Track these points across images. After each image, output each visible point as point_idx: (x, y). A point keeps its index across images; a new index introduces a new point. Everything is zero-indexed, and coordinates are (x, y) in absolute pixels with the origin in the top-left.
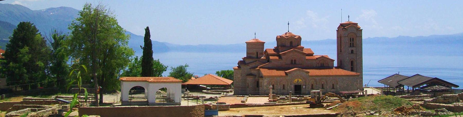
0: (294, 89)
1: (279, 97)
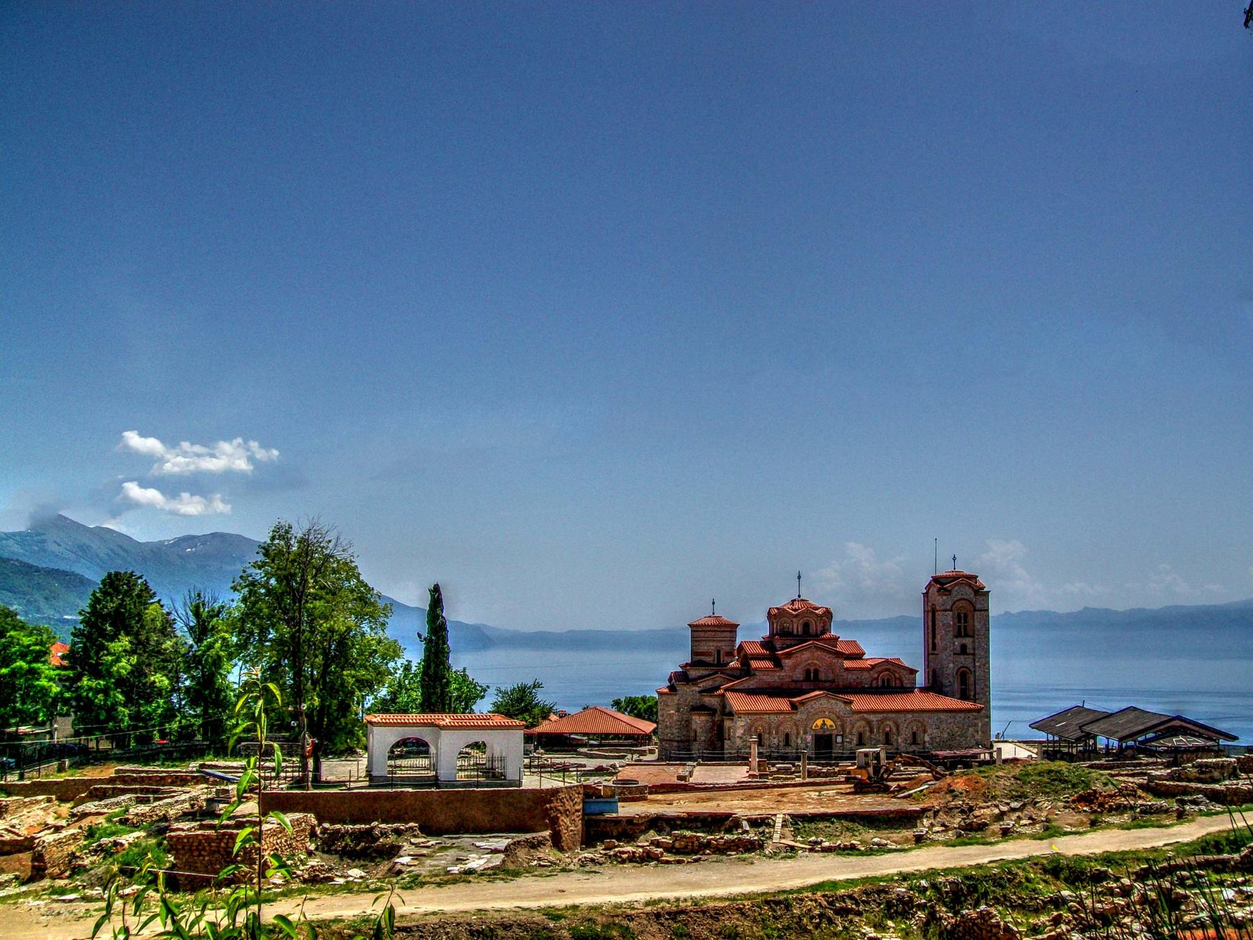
1: (773, 765)
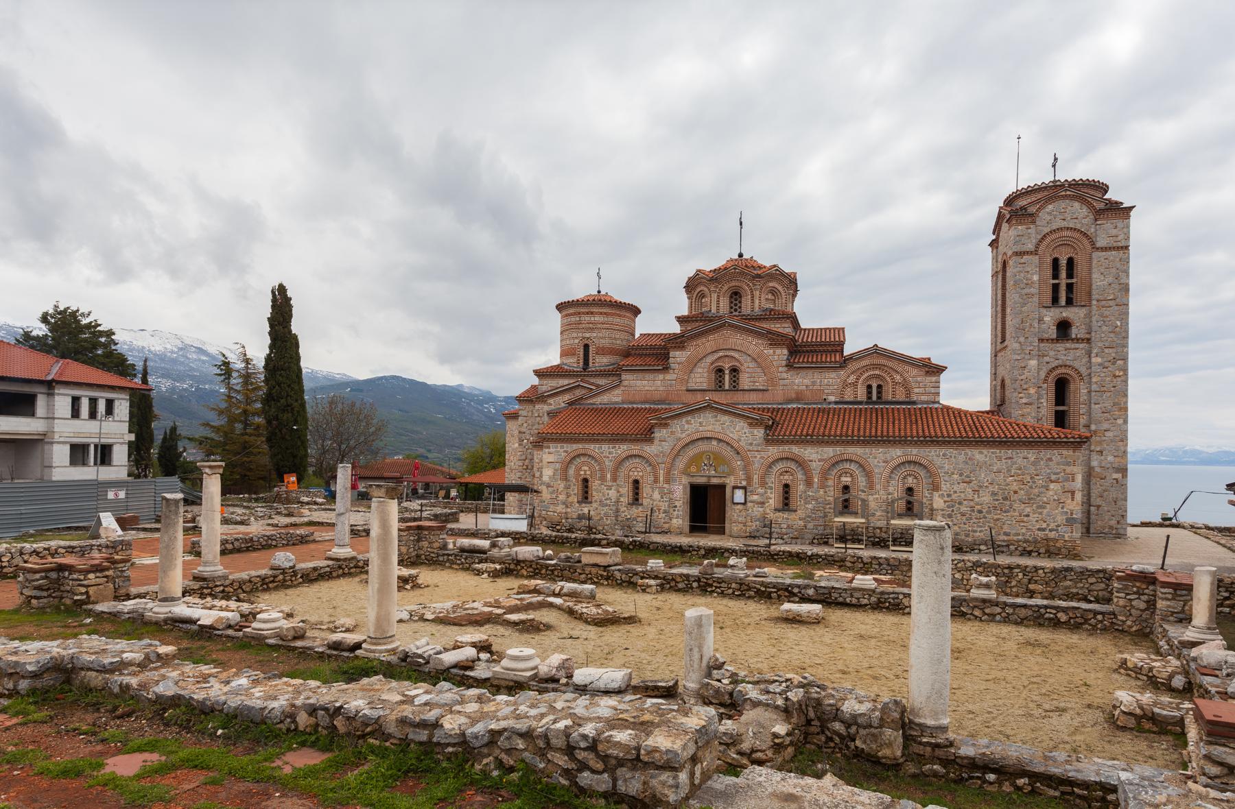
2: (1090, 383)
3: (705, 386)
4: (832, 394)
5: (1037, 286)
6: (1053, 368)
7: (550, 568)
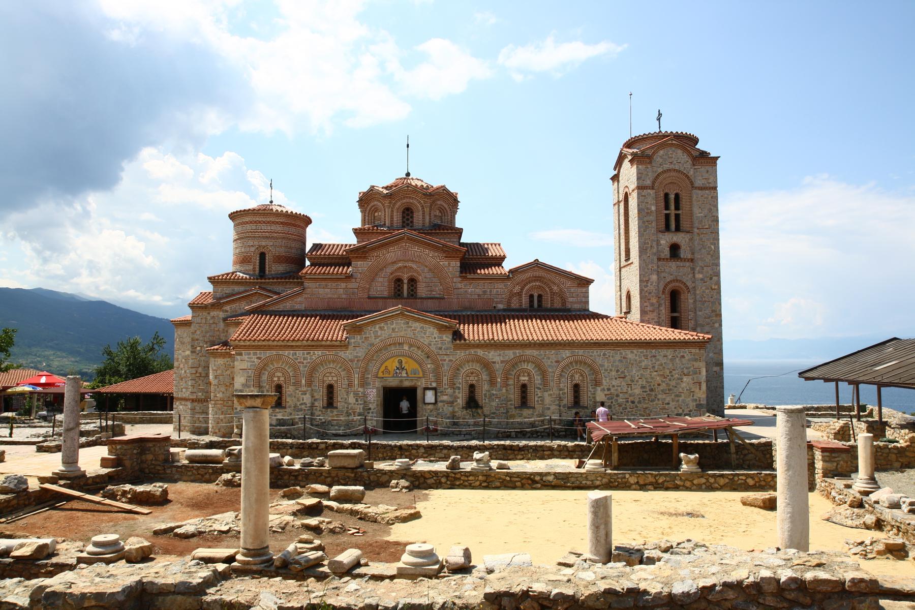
0: (380, 410)
2: (695, 294)
3: (386, 294)
4: (500, 302)
5: (655, 214)
6: (669, 282)
7: (292, 474)
